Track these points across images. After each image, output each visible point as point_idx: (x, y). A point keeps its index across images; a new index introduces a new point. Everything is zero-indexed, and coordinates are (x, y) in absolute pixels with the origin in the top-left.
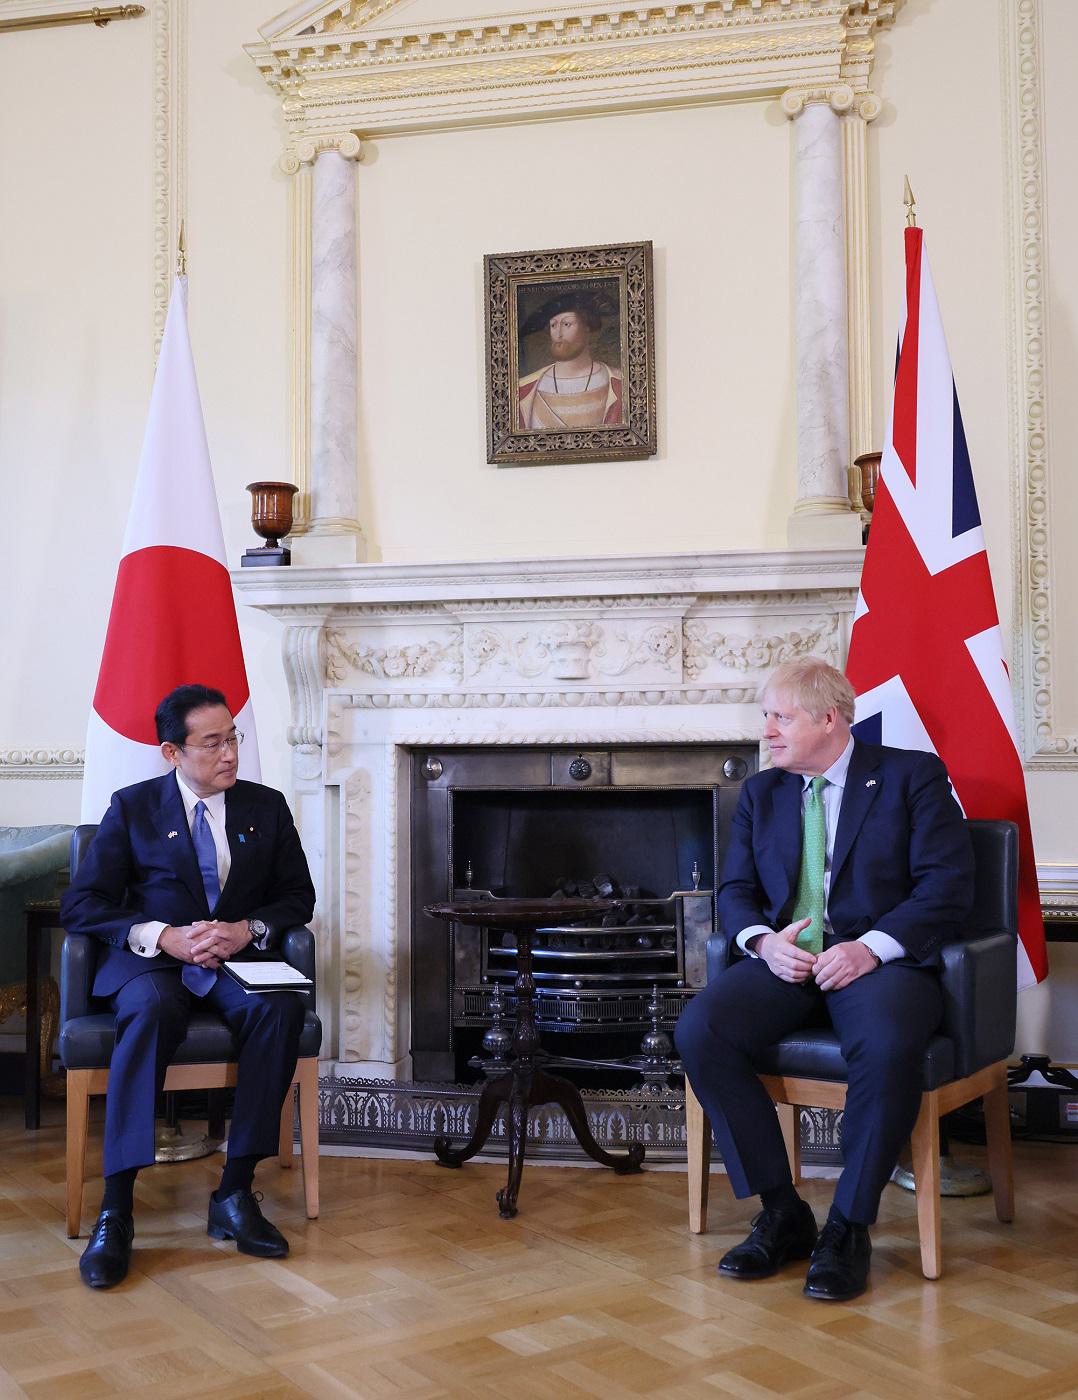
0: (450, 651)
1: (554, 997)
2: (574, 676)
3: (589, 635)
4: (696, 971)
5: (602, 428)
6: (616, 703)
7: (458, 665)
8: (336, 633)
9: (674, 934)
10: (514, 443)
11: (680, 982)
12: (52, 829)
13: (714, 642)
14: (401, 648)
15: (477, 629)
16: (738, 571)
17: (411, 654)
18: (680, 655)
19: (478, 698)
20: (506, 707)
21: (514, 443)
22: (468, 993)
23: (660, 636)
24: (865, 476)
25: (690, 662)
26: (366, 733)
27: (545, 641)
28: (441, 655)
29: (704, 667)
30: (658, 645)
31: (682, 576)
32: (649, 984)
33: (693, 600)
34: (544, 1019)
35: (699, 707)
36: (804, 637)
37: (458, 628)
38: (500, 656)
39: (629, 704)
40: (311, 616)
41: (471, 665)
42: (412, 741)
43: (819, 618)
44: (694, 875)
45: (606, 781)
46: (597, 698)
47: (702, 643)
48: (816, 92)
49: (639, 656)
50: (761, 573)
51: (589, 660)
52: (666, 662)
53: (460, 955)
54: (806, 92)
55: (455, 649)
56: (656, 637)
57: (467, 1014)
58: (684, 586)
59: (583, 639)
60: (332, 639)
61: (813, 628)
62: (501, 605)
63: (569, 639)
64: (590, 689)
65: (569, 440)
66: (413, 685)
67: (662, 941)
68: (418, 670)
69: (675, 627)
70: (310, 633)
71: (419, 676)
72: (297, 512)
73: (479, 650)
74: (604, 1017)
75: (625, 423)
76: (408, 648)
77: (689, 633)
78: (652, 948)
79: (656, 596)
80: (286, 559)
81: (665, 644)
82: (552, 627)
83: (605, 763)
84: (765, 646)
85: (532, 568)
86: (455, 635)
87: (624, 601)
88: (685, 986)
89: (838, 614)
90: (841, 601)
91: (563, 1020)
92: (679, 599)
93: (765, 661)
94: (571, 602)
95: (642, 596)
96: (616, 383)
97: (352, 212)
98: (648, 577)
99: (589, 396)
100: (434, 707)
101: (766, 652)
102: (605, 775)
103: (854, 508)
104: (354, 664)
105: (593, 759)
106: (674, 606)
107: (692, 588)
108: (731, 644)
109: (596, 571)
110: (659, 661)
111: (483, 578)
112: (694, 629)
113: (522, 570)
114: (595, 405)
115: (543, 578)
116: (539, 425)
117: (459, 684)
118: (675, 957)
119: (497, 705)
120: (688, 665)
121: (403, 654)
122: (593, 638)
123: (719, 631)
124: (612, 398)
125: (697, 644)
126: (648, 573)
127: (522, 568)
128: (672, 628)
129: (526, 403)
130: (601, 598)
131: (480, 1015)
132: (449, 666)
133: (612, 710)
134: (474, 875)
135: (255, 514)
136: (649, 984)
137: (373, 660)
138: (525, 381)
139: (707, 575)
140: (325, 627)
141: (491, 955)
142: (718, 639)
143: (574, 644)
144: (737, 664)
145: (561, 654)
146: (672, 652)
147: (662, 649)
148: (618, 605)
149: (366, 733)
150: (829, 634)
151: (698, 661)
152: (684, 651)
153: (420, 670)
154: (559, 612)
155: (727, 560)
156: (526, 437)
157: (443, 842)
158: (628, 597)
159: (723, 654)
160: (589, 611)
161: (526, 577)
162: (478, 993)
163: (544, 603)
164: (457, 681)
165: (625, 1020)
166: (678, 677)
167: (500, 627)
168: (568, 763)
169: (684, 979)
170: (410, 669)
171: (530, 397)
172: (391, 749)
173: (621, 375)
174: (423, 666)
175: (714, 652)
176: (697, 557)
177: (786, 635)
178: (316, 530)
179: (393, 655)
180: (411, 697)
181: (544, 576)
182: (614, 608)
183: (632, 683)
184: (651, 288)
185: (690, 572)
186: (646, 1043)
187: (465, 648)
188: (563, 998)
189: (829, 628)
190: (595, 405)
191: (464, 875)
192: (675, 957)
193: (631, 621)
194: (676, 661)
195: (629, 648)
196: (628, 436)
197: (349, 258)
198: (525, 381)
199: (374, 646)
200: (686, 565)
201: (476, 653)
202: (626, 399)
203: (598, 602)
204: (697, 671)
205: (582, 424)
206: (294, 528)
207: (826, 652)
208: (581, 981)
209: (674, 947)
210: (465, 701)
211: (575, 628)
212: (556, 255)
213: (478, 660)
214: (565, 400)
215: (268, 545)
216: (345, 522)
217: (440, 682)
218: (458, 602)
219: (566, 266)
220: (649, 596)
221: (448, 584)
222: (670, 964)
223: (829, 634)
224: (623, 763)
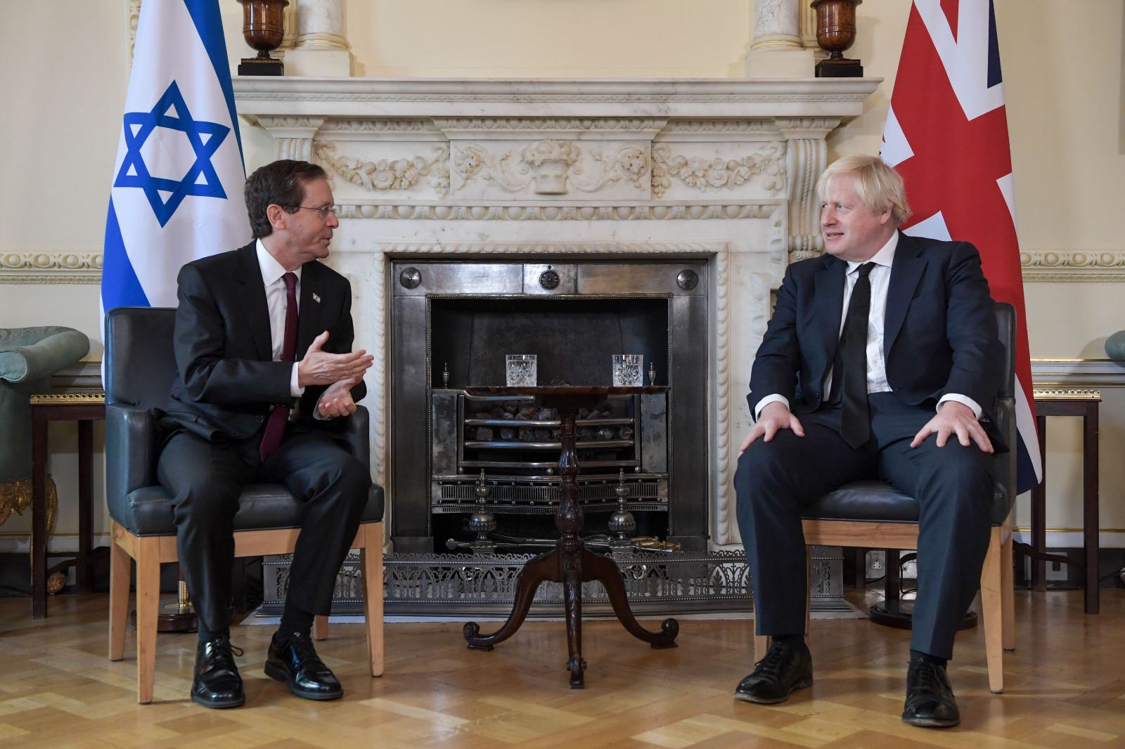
0: (434, 167)
1: (527, 484)
2: (555, 190)
3: (569, 154)
4: (651, 457)
6: (589, 218)
7: (444, 179)
8: (325, 146)
9: (632, 426)
11: (637, 469)
12: (47, 331)
13: (679, 163)
14: (390, 160)
15: (463, 146)
16: (707, 98)
17: (399, 167)
18: (649, 175)
19: (464, 209)
20: (488, 219)
22: (445, 482)
23: (633, 157)
24: (820, 17)
26: (354, 242)
27: (530, 158)
29: (669, 186)
30: (631, 165)
31: (657, 101)
32: (616, 470)
33: (664, 123)
34: (517, 503)
35: (664, 224)
36: (758, 160)
37: (443, 145)
38: (484, 172)
39: (601, 218)
40: (302, 128)
41: (456, 180)
43: (772, 145)
44: (651, 373)
45: (572, 290)
46: (574, 212)
47: (668, 165)
49: (612, 175)
50: (729, 101)
51: (567, 178)
52: (638, 180)
53: (436, 449)
55: (440, 165)
56: (629, 157)
57: (444, 502)
58: (660, 110)
59: (565, 157)
60: (320, 152)
61: (766, 153)
62: (488, 123)
63: (553, 156)
64: (570, 204)
67: (621, 432)
68: (405, 183)
69: (646, 148)
70: (302, 144)
71: (405, 189)
72: (287, 26)
73: (465, 166)
74: (554, 501)
76: (397, 161)
77: (656, 156)
78: (612, 439)
79: (630, 119)
80: (276, 69)
81: (637, 164)
82: (537, 145)
83: (572, 274)
84: (724, 168)
85: (523, 88)
86: (440, 151)
87: (602, 123)
88: (641, 471)
89: (786, 141)
90: (793, 130)
91: (536, 504)
92: (651, 123)
93: (723, 182)
94: (553, 123)
95: (618, 119)
98: (628, 101)
100: (419, 217)
101: (725, 173)
102: (571, 285)
103: (802, 46)
104: (343, 175)
105: (562, 270)
106: (646, 130)
107: (667, 113)
109: (582, 94)
110: (632, 179)
111: (475, 96)
112: (660, 152)
113: (512, 89)
115: (530, 98)
117: (443, 198)
118: (632, 448)
119: (480, 218)
120: (656, 184)
122: (573, 156)
123: (684, 155)
125: (664, 167)
126: (629, 97)
128: (642, 149)
130: (581, 119)
131: (456, 502)
132: (434, 180)
133: (585, 223)
134: (450, 376)
135: (247, 23)
136: (616, 470)
137: (362, 173)
139: (679, 101)
140: (314, 140)
141: (466, 449)
142: (683, 161)
143: (556, 162)
144: (699, 183)
145: (545, 171)
146: (643, 171)
147: (635, 169)
148: (596, 127)
149: (354, 242)
150: (779, 159)
151: (665, 182)
152: (652, 172)
153: (407, 183)
154: (541, 132)
155: (700, 88)
157: (420, 345)
158: (606, 119)
159: (687, 175)
160: (568, 131)
161: (515, 97)
162: (454, 482)
163: (528, 122)
164: (441, 195)
165: (590, 502)
166: (647, 194)
167: (483, 144)
168: (534, 273)
169: (641, 466)
170: (398, 182)
172: (380, 257)
174: (410, 179)
175: (678, 173)
176: (674, 83)
177: (743, 159)
178: (308, 44)
179: (382, 168)
180: (400, 209)
181: (533, 96)
182: (591, 130)
183: (605, 199)
186: (615, 521)
187: (451, 165)
188: (536, 484)
189: (779, 153)
191: (442, 377)
192: (632, 448)
193: (605, 143)
194: (645, 180)
195: (600, 167)
199: (363, 159)
200: (664, 90)
201: (463, 168)
203: (578, 123)
204: (663, 190)
206: (285, 43)
207: (775, 175)
208: (553, 468)
209: (632, 437)
210: (451, 213)
211: (555, 145)
213: (464, 175)
215: (260, 56)
216: (335, 38)
217: (427, 195)
218: (447, 118)
220: (624, 118)
221: (442, 101)
222: (628, 453)
223: (779, 159)
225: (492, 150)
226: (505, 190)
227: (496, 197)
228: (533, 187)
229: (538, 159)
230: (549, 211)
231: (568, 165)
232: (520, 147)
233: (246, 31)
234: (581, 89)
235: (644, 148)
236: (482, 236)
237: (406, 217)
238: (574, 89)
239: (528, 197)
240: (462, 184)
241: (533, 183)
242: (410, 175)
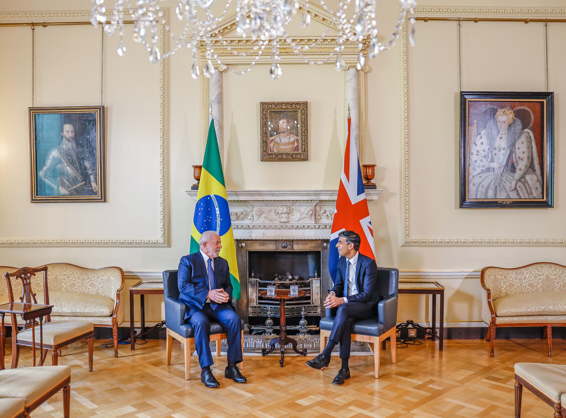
5: (293, 152)
10: (268, 155)
15: (258, 208)
17: (238, 214)
21: (268, 155)
25: (317, 217)
28: (247, 215)
35: (319, 230)
38: (264, 215)
39: (300, 229)
41: (256, 218)
42: (239, 238)
48: (352, 65)
49: (303, 216)
54: (349, 65)
65: (284, 156)
66: (240, 223)
75: (300, 151)
85: (275, 193)
96: (297, 140)
97: (221, 87)
99: (289, 143)
108: (328, 213)
111: (261, 195)
113: (272, 193)
114: (291, 146)
116: (275, 151)
121: (236, 214)
124: (296, 144)
126: (307, 195)
127: (272, 193)
129: (272, 145)
133: (295, 230)
138: (271, 139)
145: (282, 216)
147: (309, 215)
151: (319, 218)
156: (272, 154)
160: (289, 204)
166: (313, 222)
167: (264, 207)
171: (273, 143)
173: (299, 138)
183: (301, 223)
184: (307, 115)
185: (318, 195)
187: (254, 213)
190: (291, 146)
194: (313, 217)
196: (300, 154)
197: (220, 100)
198: (271, 139)
200: (317, 193)
202: (300, 145)
205: (288, 151)
212: (281, 104)
214: (282, 145)
217: (247, 222)
219: (284, 107)
224: (297, 244)
225: (266, 209)
226: (270, 220)
227: (267, 222)
228: (278, 220)
229: (280, 212)
230: (285, 227)
231: (289, 213)
232: (275, 208)
233: (195, 176)
234: (292, 193)
235: (313, 208)
236: (263, 234)
237: (240, 229)
238: (291, 192)
239: (277, 223)
240: (257, 218)
241: (278, 220)
242: (242, 216)
